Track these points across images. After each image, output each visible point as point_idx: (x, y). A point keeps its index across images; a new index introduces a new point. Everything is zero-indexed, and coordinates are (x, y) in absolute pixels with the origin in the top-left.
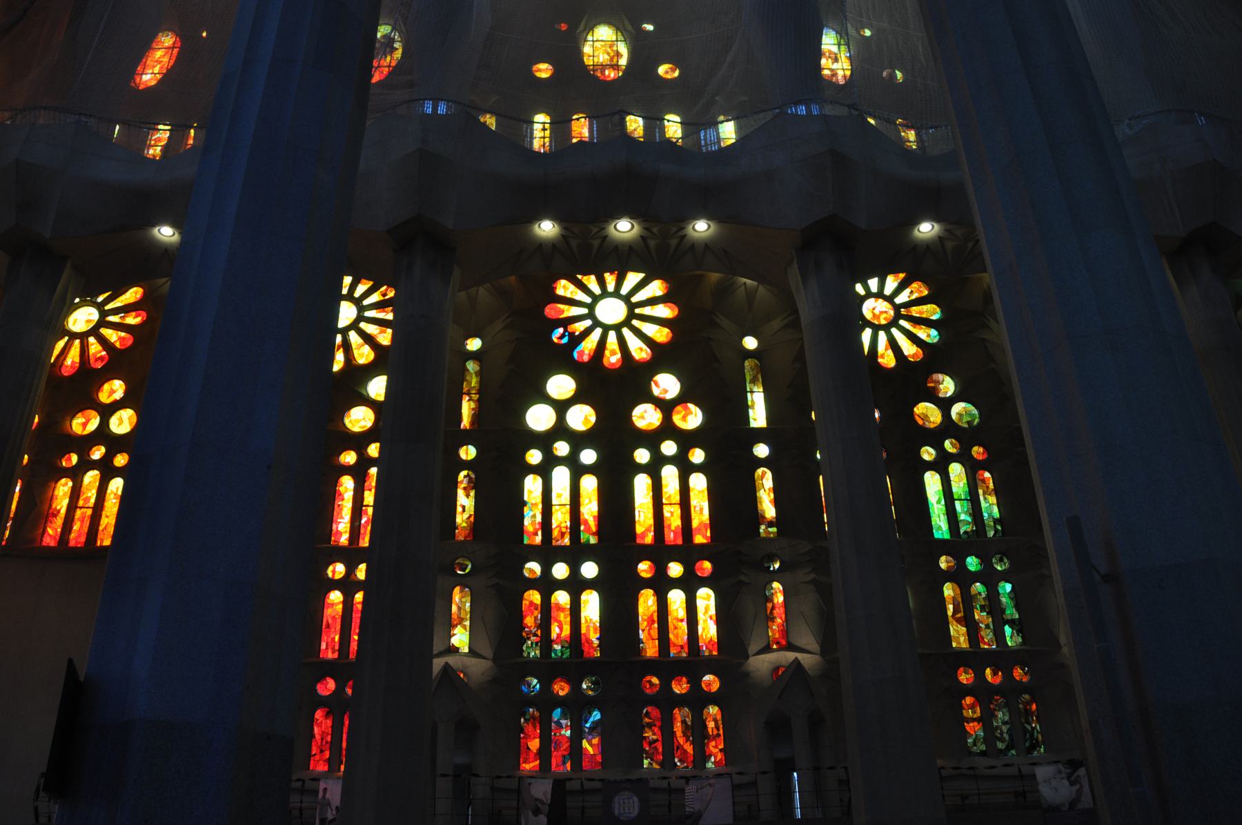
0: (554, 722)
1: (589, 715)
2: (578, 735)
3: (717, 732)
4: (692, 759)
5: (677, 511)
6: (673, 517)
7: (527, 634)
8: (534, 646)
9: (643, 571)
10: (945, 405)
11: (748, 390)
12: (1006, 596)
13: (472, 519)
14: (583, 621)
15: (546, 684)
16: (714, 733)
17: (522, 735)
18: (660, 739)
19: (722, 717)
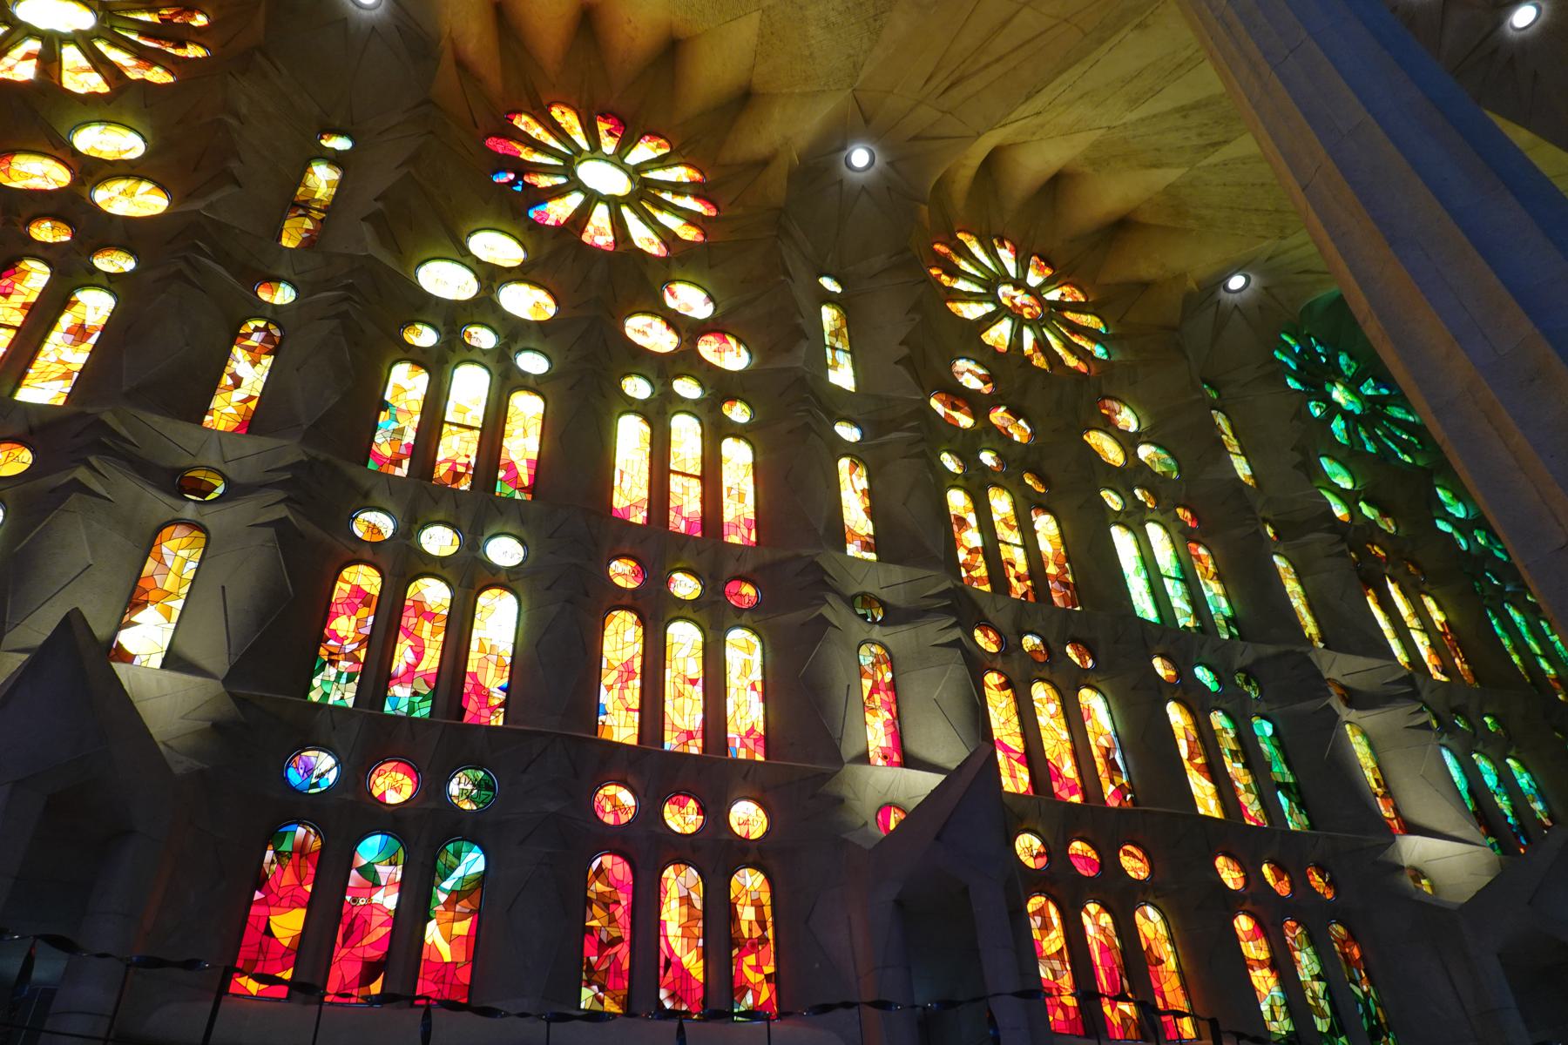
0: (358, 870)
1: (456, 861)
2: (415, 908)
3: (760, 933)
4: (699, 995)
5: (695, 487)
6: (686, 499)
7: (331, 654)
8: (343, 680)
9: (619, 574)
10: (1128, 442)
11: (827, 343)
12: (1268, 741)
13: (253, 405)
14: (474, 645)
15: (356, 772)
16: (755, 935)
17: (258, 895)
18: (627, 938)
19: (773, 897)
